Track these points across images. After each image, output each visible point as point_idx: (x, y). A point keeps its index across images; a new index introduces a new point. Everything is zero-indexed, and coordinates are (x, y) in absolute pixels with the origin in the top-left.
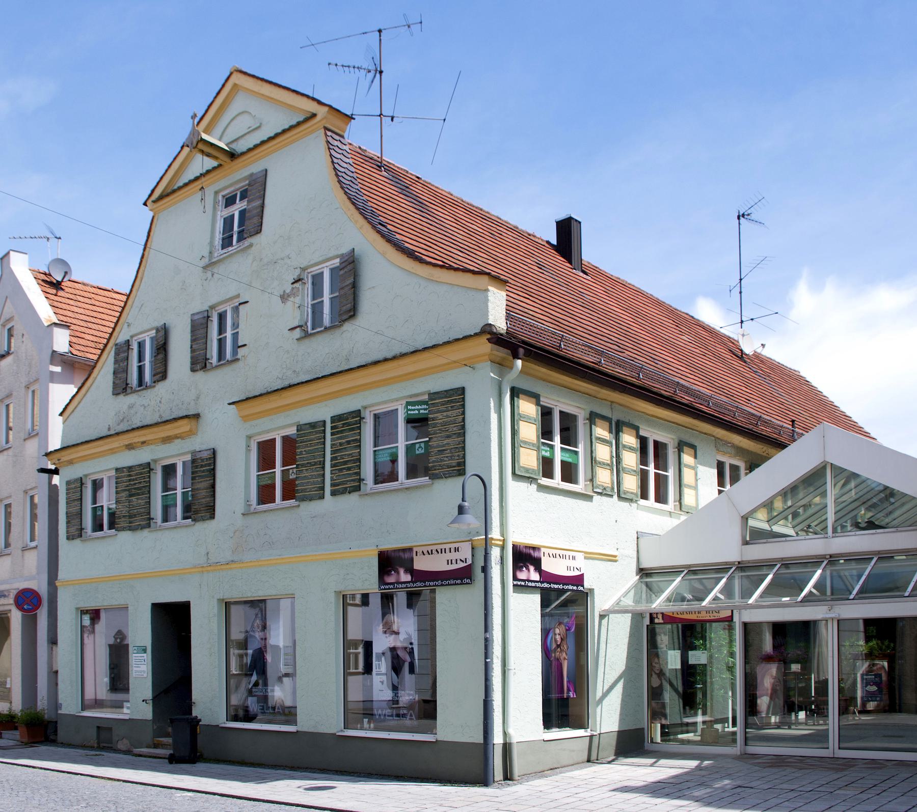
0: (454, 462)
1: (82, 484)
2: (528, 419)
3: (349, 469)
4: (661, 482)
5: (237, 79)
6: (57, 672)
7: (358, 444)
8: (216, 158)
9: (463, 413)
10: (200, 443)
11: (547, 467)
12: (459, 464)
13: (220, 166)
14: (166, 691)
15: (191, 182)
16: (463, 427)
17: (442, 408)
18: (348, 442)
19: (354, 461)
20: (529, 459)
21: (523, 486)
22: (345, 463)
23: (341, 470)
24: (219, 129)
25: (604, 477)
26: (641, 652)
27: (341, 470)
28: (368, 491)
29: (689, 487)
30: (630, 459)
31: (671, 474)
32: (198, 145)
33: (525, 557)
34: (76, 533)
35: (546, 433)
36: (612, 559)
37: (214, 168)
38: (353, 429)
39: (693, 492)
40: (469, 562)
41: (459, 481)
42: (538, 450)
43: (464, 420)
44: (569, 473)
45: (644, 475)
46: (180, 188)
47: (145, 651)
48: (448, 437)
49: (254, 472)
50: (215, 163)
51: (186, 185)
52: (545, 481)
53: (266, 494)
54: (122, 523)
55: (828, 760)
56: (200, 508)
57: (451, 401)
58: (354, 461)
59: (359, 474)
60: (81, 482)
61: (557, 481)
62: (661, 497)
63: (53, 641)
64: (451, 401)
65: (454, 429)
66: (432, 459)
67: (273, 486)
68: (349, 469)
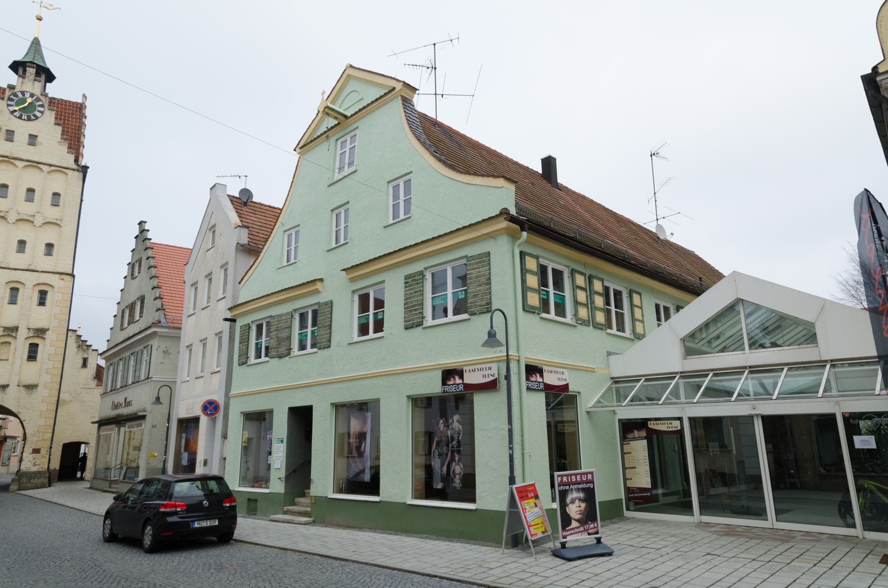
0: (484, 303)
1: (250, 328)
2: (531, 272)
3: (416, 310)
4: (620, 317)
5: (351, 72)
6: (225, 459)
7: (422, 292)
8: (336, 118)
9: (490, 269)
10: (322, 298)
11: (545, 304)
12: (487, 304)
13: (339, 123)
14: (294, 471)
15: (322, 134)
16: (489, 279)
17: (475, 266)
18: (416, 292)
19: (419, 305)
20: (534, 300)
21: (530, 316)
22: (414, 306)
23: (411, 311)
24: (339, 102)
25: (583, 313)
26: (615, 439)
27: (411, 311)
28: (429, 324)
29: (639, 320)
30: (599, 301)
31: (626, 311)
32: (328, 111)
33: (532, 370)
34: (243, 362)
35: (544, 283)
36: (591, 371)
37: (336, 125)
38: (418, 283)
39: (641, 324)
40: (496, 376)
41: (489, 315)
42: (539, 294)
43: (490, 273)
44: (560, 310)
45: (608, 313)
46: (315, 139)
47: (282, 442)
48: (480, 285)
49: (356, 315)
50: (336, 122)
51: (318, 137)
52: (544, 315)
53: (363, 330)
54: (273, 353)
55: (770, 531)
56: (322, 343)
57: (482, 262)
58: (419, 305)
59: (422, 313)
60: (249, 327)
61: (552, 315)
62: (621, 328)
63: (225, 437)
64: (482, 262)
65: (483, 280)
66: (469, 301)
67: (368, 324)
68: (416, 310)
